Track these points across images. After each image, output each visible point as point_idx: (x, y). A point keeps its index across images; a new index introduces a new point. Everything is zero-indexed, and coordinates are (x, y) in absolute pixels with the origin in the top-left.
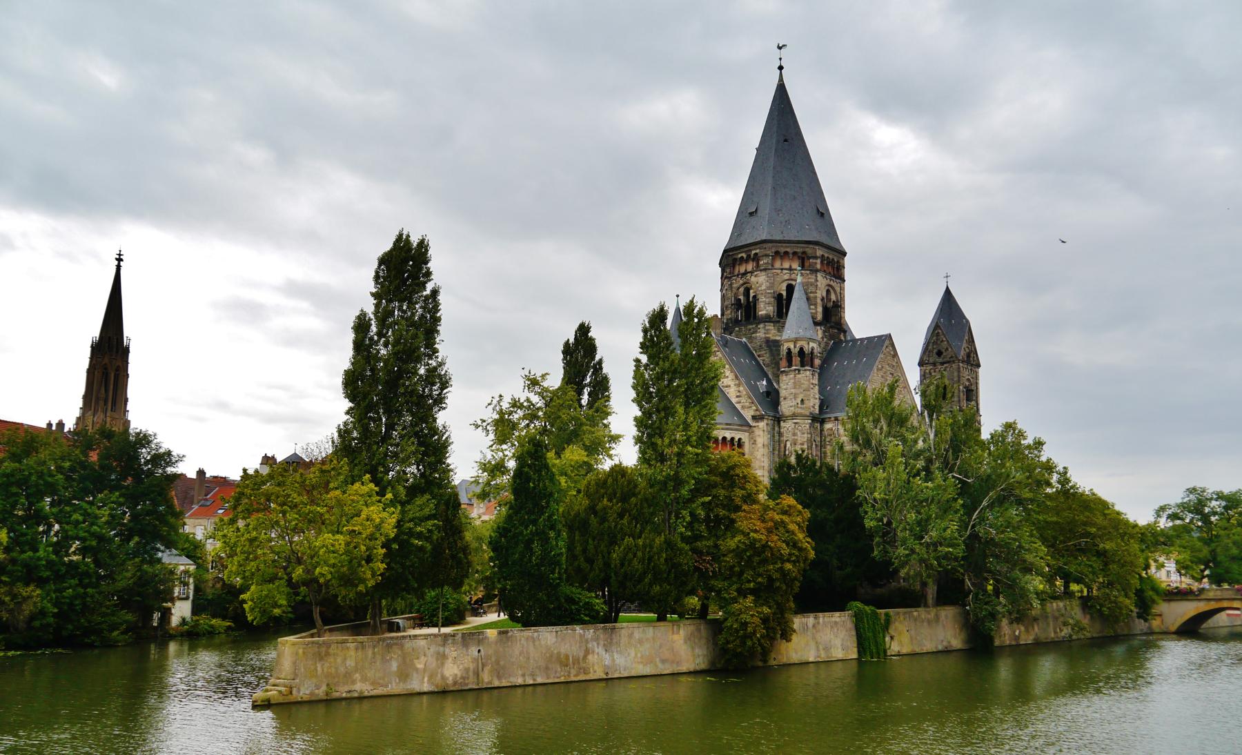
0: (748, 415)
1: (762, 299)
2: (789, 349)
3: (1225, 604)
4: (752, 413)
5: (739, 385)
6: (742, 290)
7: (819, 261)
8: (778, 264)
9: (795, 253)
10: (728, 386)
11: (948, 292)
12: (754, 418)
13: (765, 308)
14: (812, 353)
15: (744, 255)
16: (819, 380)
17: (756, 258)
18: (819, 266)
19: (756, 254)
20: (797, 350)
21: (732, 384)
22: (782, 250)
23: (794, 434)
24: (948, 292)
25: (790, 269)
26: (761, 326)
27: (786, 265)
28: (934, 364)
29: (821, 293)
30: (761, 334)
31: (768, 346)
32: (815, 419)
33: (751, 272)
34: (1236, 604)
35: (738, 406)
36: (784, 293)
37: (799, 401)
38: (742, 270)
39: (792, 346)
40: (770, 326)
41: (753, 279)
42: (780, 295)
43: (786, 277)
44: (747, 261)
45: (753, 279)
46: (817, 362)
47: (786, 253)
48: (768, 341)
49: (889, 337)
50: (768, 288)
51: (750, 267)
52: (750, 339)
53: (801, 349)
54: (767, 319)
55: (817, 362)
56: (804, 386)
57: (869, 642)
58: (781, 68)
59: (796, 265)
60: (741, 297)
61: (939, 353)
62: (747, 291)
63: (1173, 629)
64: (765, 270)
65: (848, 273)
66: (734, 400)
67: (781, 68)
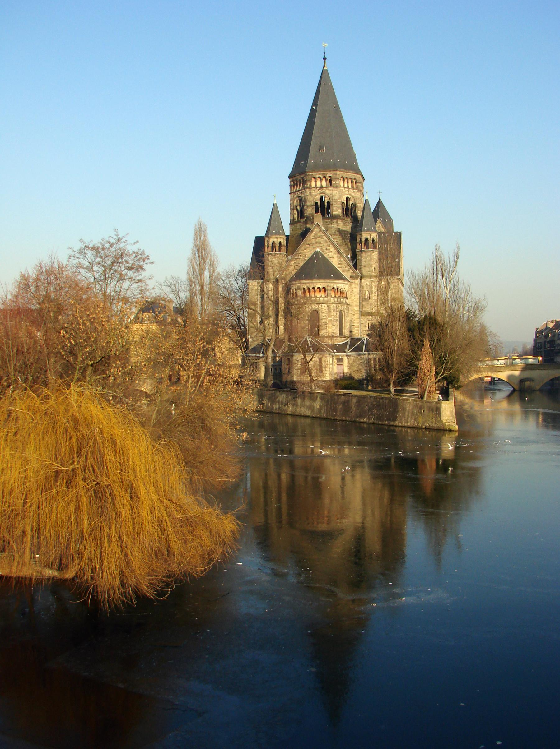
0: (347, 275)
4: (350, 274)
5: (340, 258)
6: (318, 197)
10: (332, 257)
12: (351, 277)
13: (337, 210)
20: (371, 239)
21: (335, 256)
22: (345, 177)
23: (371, 287)
26: (335, 221)
27: (346, 186)
37: (373, 268)
38: (319, 184)
39: (368, 237)
40: (340, 222)
41: (328, 192)
42: (343, 203)
44: (321, 180)
49: (400, 233)
50: (339, 198)
54: (336, 217)
58: (325, 59)
59: (350, 187)
64: (337, 187)
66: (336, 266)
67: (325, 59)
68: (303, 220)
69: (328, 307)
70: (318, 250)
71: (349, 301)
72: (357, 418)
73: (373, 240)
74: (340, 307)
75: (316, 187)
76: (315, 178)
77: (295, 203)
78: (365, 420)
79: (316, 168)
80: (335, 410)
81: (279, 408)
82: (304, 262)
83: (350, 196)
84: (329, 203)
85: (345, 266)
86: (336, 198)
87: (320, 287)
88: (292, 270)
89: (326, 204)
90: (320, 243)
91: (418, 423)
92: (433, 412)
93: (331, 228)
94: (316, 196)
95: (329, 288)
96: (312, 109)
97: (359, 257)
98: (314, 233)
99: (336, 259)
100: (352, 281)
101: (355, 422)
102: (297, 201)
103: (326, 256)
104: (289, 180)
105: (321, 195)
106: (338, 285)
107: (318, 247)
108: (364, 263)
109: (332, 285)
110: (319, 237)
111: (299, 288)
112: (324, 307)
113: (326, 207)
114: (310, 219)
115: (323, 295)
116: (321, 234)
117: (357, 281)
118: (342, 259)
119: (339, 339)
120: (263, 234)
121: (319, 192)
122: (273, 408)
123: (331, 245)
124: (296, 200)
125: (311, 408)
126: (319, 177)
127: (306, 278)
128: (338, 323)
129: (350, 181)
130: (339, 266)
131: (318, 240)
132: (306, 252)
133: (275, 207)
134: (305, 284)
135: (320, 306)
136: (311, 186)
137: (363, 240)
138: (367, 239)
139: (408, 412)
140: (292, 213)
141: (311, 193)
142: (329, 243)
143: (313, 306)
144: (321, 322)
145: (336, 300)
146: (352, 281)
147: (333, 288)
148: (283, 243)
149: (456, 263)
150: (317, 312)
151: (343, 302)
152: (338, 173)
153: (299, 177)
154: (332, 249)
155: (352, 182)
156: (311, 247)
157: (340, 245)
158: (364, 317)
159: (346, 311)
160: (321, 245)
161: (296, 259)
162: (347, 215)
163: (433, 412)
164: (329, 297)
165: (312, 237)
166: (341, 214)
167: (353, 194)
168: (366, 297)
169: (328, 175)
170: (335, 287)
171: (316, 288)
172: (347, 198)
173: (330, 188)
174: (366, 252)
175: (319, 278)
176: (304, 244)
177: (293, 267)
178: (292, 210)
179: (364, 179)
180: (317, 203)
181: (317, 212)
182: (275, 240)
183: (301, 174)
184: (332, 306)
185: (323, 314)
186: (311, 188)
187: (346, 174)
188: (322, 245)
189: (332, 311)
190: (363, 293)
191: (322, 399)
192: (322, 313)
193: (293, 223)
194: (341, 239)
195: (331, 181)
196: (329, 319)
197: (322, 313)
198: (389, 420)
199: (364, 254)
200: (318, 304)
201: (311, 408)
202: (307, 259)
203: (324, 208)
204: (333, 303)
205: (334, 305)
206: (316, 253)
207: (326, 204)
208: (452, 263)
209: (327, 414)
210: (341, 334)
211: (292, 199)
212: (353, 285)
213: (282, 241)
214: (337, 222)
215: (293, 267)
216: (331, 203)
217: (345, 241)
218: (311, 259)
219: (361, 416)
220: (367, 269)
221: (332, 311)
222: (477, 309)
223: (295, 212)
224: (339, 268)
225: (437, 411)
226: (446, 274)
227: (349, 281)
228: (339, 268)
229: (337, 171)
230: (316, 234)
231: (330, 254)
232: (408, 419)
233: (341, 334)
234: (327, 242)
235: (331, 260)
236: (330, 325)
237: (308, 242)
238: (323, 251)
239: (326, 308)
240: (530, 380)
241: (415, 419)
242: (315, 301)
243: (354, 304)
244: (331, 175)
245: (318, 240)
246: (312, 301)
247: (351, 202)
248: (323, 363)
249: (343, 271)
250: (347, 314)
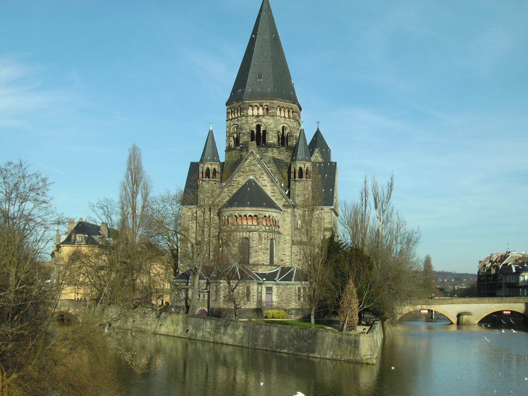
0: (280, 204)
1: (271, 133)
2: (301, 168)
5: (273, 186)
6: (254, 125)
8: (278, 113)
12: (284, 206)
13: (272, 139)
15: (258, 105)
20: (306, 169)
21: (269, 185)
25: (285, 117)
26: (270, 149)
27: (283, 115)
30: (270, 154)
35: (273, 199)
36: (281, 132)
39: (303, 166)
41: (264, 120)
42: (279, 132)
43: (283, 122)
45: (264, 120)
49: (335, 163)
50: (275, 127)
54: (272, 146)
59: (287, 116)
62: (258, 127)
64: (273, 116)
66: (269, 194)
68: (238, 148)
69: (259, 235)
70: (251, 177)
71: (281, 230)
72: (278, 348)
73: (307, 170)
74: (271, 236)
75: (253, 116)
76: (252, 106)
77: (232, 131)
78: (286, 351)
79: (254, 96)
80: (256, 339)
81: (202, 336)
82: (237, 189)
83: (286, 126)
84: (264, 132)
86: (272, 126)
87: (252, 214)
88: (226, 197)
89: (261, 132)
90: (254, 171)
91: (337, 356)
92: (351, 345)
93: (266, 156)
95: (261, 216)
96: (251, 37)
97: (292, 186)
98: (248, 160)
99: (268, 188)
100: (284, 210)
101: (276, 352)
102: (234, 128)
103: (259, 184)
104: (226, 107)
105: (257, 123)
106: (270, 213)
107: (252, 175)
108: (297, 192)
109: (264, 213)
110: (253, 165)
111: (231, 215)
112: (255, 235)
113: (262, 135)
114: (245, 147)
115: (255, 223)
116: (255, 162)
117: (290, 210)
118: (275, 188)
119: (269, 268)
120: (198, 160)
121: (255, 120)
122: (197, 336)
123: (265, 174)
124: (232, 127)
125: (233, 336)
126: (256, 106)
127: (239, 205)
128: (269, 251)
129: (287, 110)
130: (272, 194)
131: (252, 167)
132: (240, 180)
133: (211, 134)
134: (236, 211)
135: (251, 234)
136: (247, 114)
137: (297, 169)
139: (327, 344)
140: (228, 140)
141: (247, 121)
142: (263, 171)
143: (245, 234)
144: (251, 251)
145: (267, 228)
146: (284, 210)
147: (265, 216)
148: (217, 170)
149: (390, 194)
150: (247, 239)
151: (274, 231)
152: (275, 102)
153: (235, 104)
154: (265, 177)
155: (289, 111)
156: (245, 175)
157: (275, 174)
158: (295, 246)
159: (277, 240)
160: (255, 173)
161: (229, 186)
162: (283, 144)
163: (351, 345)
164: (261, 226)
165: (246, 165)
166: (276, 143)
167: (289, 123)
168: (299, 227)
169: (264, 104)
170: (267, 215)
171: (248, 216)
172: (283, 127)
173: (266, 117)
174: (299, 182)
175: (251, 206)
176: (238, 172)
177: (226, 194)
178: (229, 137)
179: (301, 109)
180: (253, 131)
181: (252, 141)
182: (210, 167)
183: (237, 101)
184: (263, 235)
185: (254, 242)
186: (247, 116)
187: (282, 104)
188: (255, 173)
189: (263, 239)
191: (244, 327)
192: (253, 241)
193: (229, 149)
194: (275, 167)
195: (267, 109)
196: (260, 247)
197: (253, 241)
198: (308, 351)
199: (297, 184)
200: (249, 232)
201: (233, 336)
202: (240, 186)
203: (259, 137)
204: (264, 231)
205: (265, 233)
206: (250, 181)
207: (261, 132)
208: (386, 194)
209: (249, 343)
210: (272, 263)
211: (229, 127)
212: (286, 214)
213: (216, 167)
214: (272, 151)
215: (226, 194)
216: (267, 132)
217: (279, 170)
218: (245, 186)
219: (281, 347)
221: (263, 239)
222: (410, 241)
223: (232, 139)
224: (273, 196)
225: (356, 344)
226: (379, 205)
228: (273, 196)
229: (273, 100)
230: (250, 162)
232: (327, 351)
233: (272, 263)
234: (261, 171)
235: (264, 188)
236: (261, 253)
237: (241, 170)
238: (257, 179)
239: (258, 236)
240: (468, 314)
241: (334, 352)
242: (246, 228)
243: (286, 233)
244: (268, 104)
245: (252, 167)
246: (243, 228)
247: (286, 132)
248: (251, 291)
249: (276, 199)
250: (279, 243)
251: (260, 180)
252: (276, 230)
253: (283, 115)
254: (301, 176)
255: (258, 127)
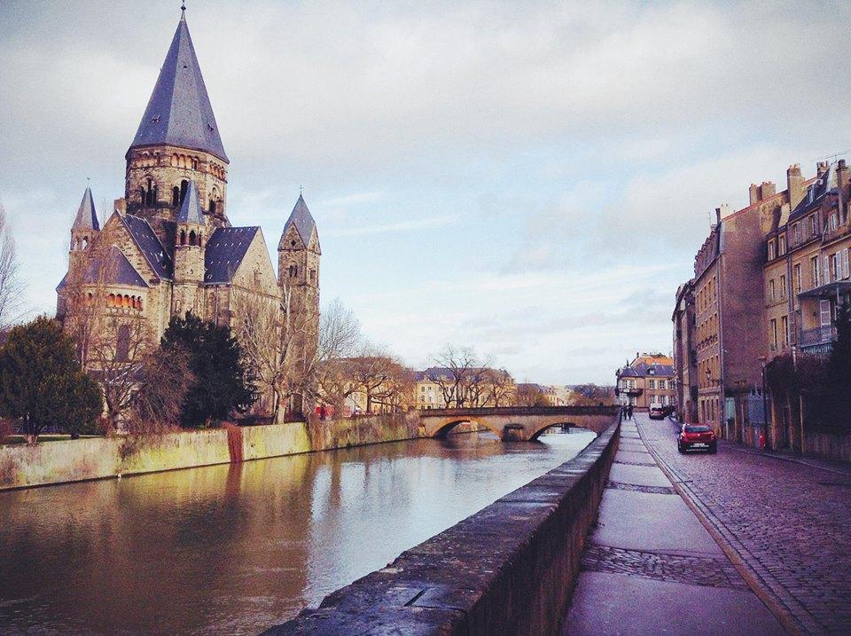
0: (146, 278)
3: (462, 418)
6: (144, 180)
7: (208, 166)
8: (174, 163)
9: (190, 157)
11: (301, 199)
12: (151, 281)
13: (166, 196)
14: (200, 236)
15: (148, 153)
16: (205, 257)
17: (159, 157)
18: (208, 169)
19: (158, 153)
20: (189, 232)
22: (179, 153)
24: (301, 199)
25: (185, 168)
27: (182, 165)
28: (289, 250)
29: (209, 190)
30: (158, 217)
31: (165, 227)
32: (200, 285)
33: (153, 167)
34: (468, 418)
36: (180, 187)
38: (145, 165)
42: (176, 188)
43: (182, 174)
44: (148, 157)
46: (204, 242)
47: (182, 155)
48: (164, 222)
51: (151, 162)
52: (150, 219)
53: (192, 231)
54: (163, 205)
55: (204, 242)
56: (193, 260)
57: (235, 446)
58: (183, 8)
59: (189, 166)
60: (146, 188)
61: (293, 243)
63: (431, 435)
65: (228, 177)
66: (135, 266)
67: (183, 8)
70: (115, 245)
75: (142, 168)
83: (188, 180)
85: (145, 268)
94: (141, 178)
110: (118, 228)
116: (120, 225)
118: (142, 258)
138: (183, 234)
145: (114, 310)
147: (112, 295)
169: (156, 151)
170: (115, 294)
174: (180, 249)
190: (174, 303)
214: (162, 212)
220: (181, 272)
227: (146, 286)
231: (130, 252)
235: (129, 258)
245: (118, 232)
249: (143, 273)
251: (125, 247)
252: (131, 313)
253: (182, 165)
254: (183, 242)
255: (150, 181)
